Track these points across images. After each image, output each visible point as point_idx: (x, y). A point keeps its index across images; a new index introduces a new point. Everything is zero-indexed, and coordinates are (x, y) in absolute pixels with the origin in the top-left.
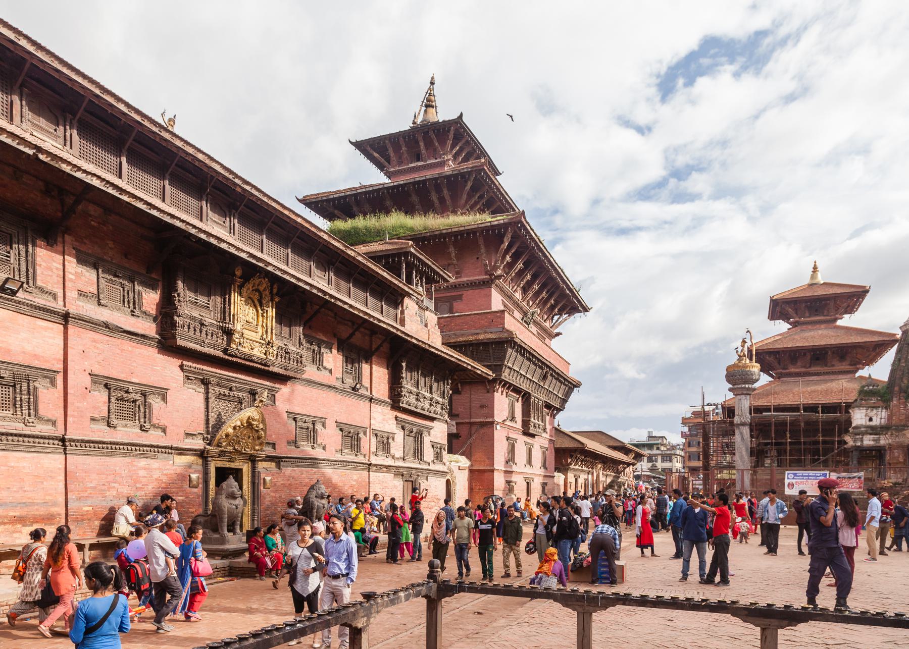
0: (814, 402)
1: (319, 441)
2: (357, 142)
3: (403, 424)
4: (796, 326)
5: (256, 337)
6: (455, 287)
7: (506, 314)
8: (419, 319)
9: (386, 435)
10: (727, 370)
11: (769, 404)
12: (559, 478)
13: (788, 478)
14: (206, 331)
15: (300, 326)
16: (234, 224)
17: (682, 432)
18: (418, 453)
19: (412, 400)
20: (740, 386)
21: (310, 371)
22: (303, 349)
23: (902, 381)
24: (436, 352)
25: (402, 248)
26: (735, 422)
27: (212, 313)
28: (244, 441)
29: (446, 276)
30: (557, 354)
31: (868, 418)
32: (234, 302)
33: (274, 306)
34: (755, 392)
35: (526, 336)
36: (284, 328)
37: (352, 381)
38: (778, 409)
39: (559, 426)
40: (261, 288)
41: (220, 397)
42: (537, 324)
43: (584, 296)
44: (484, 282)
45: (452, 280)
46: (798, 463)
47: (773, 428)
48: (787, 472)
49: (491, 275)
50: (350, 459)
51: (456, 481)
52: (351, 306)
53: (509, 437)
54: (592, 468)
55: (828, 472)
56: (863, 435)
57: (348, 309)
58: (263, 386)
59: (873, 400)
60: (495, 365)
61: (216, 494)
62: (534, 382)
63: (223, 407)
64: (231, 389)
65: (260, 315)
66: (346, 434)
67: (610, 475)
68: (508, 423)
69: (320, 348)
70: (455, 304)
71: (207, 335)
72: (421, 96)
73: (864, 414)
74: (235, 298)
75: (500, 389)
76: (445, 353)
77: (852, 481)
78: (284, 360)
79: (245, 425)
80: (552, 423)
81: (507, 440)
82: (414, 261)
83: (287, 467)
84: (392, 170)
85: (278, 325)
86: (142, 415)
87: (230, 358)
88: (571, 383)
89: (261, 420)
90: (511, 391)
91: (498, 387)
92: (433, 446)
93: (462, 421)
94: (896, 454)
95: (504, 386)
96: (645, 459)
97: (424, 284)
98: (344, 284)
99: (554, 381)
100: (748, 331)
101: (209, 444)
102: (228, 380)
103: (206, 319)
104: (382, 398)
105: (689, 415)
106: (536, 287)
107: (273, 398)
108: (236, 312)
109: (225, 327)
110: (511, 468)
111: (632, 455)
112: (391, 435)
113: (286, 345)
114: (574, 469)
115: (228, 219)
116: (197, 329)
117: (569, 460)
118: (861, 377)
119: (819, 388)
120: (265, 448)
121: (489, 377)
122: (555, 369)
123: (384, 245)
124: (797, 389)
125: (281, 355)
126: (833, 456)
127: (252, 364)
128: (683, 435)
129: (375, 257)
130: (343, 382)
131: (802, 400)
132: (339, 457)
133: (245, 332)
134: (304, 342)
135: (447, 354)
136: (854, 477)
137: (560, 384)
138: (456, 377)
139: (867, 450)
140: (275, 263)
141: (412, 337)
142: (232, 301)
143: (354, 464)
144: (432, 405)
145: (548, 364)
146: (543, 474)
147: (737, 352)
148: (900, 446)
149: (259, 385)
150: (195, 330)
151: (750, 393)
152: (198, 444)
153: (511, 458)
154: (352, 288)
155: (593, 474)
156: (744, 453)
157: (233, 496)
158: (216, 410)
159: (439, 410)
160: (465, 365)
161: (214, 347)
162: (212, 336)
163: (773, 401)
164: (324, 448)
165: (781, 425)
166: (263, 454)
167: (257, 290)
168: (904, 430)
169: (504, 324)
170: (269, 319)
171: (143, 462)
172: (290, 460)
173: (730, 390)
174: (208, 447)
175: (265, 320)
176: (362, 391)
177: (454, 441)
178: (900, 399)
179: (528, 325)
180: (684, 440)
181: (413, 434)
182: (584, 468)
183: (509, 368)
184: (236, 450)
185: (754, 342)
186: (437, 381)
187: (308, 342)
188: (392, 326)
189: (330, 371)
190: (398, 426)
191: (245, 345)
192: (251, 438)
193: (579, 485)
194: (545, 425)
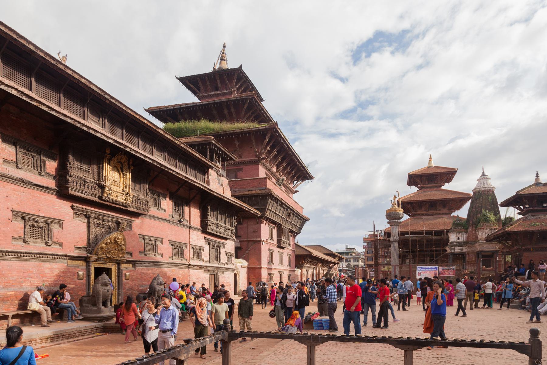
0: (430, 229)
1: (159, 252)
2: (180, 78)
3: (209, 242)
4: (421, 189)
5: (120, 190)
6: (239, 163)
7: (268, 180)
8: (218, 181)
9: (199, 248)
10: (386, 212)
11: (408, 230)
12: (298, 271)
13: (418, 270)
14: (88, 186)
15: (146, 184)
16: (105, 122)
17: (363, 246)
18: (218, 258)
19: (214, 228)
20: (393, 221)
21: (153, 211)
22: (148, 197)
23: (474, 219)
24: (228, 200)
25: (207, 141)
26: (391, 240)
27: (91, 175)
28: (112, 252)
29: (233, 157)
30: (296, 202)
31: (457, 238)
32: (106, 169)
33: (131, 172)
34: (401, 224)
35: (279, 192)
36: (137, 185)
37: (178, 217)
38: (413, 233)
39: (297, 242)
40: (122, 161)
41: (97, 225)
42: (285, 186)
43: (311, 171)
44: (255, 161)
45: (237, 159)
46: (423, 262)
47: (410, 243)
48: (417, 267)
49: (259, 157)
50: (178, 262)
51: (240, 274)
52: (177, 173)
53: (270, 249)
54: (316, 266)
55: (438, 267)
56: (455, 247)
57: (175, 174)
58: (124, 219)
59: (460, 228)
60: (261, 208)
62: (283, 218)
63: (99, 232)
64: (104, 221)
65: (122, 177)
66: (175, 247)
67: (326, 270)
68: (269, 241)
69: (159, 197)
70: (238, 173)
71: (88, 188)
72: (218, 54)
73: (455, 236)
74: (106, 166)
75: (264, 222)
76: (233, 201)
77: (450, 271)
78: (137, 204)
79: (113, 242)
80: (293, 241)
81: (269, 250)
82: (214, 148)
83: (140, 267)
84: (201, 95)
85: (133, 183)
86: (47, 236)
87: (103, 202)
88: (304, 219)
89: (123, 239)
90: (271, 223)
91: (263, 220)
92: (226, 254)
93: (243, 240)
94: (471, 257)
95: (266, 220)
96: (344, 260)
97: (220, 161)
98: (173, 160)
99: (294, 217)
100: (397, 192)
101: (90, 254)
102: (102, 215)
103: (88, 178)
104: (196, 226)
105: (367, 236)
106: (284, 165)
107: (131, 227)
108: (106, 175)
109: (100, 183)
110: (271, 266)
111: (337, 259)
112: (202, 248)
113: (138, 195)
114: (306, 267)
115: (101, 119)
116: (82, 184)
117: (303, 262)
118: (454, 216)
119: (433, 222)
120: (125, 256)
121: (258, 215)
122: (295, 210)
123: (197, 138)
124: (422, 222)
125: (135, 201)
126: (440, 258)
127: (117, 206)
128: (364, 247)
129: (192, 145)
130: (173, 217)
131: (425, 228)
132: (171, 261)
133: (112, 186)
134: (149, 193)
135: (234, 202)
136: (451, 269)
137: (298, 219)
138: (239, 215)
139: (457, 255)
140: (131, 147)
141: (214, 192)
142: (104, 168)
143: (180, 265)
144: (226, 231)
145: (291, 208)
146: (289, 269)
147: (392, 202)
148: (473, 252)
149: (121, 219)
150: (80, 185)
151: (398, 224)
152: (84, 253)
153: (271, 261)
154: (178, 162)
155: (316, 269)
156: (396, 257)
157: (106, 285)
158: (94, 233)
159: (230, 233)
160: (244, 208)
161: (93, 195)
162: (92, 189)
163: (410, 229)
164: (162, 256)
165: (414, 241)
166: (125, 259)
167: (120, 162)
168: (475, 244)
169: (266, 185)
170: (128, 180)
171: (47, 265)
172: (141, 263)
173: (388, 223)
174: (89, 255)
175: (125, 180)
176: (184, 223)
177: (239, 251)
178: (473, 228)
179: (280, 186)
180: (364, 250)
181: (215, 247)
182: (312, 266)
183: (269, 210)
184: (107, 257)
186: (228, 217)
187: (152, 193)
188: (202, 185)
189: (165, 211)
190: (206, 242)
191: (112, 194)
192: (117, 250)
193: (309, 275)
194: (290, 242)
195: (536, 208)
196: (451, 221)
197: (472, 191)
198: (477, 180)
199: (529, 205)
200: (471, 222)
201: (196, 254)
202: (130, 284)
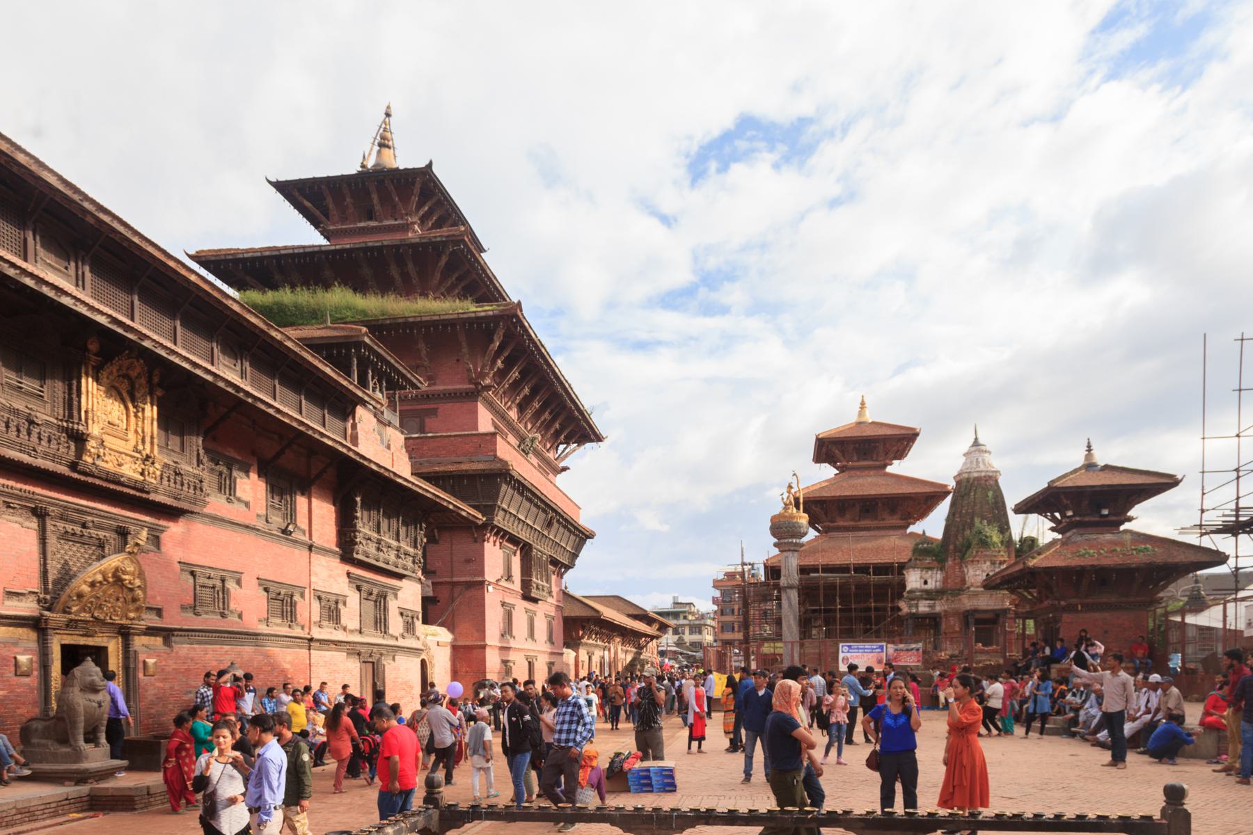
0: (865, 562)
1: (232, 606)
3: (359, 583)
4: (843, 471)
5: (128, 447)
6: (427, 397)
7: (499, 438)
8: (378, 437)
9: (334, 598)
10: (771, 520)
11: (816, 563)
12: (569, 655)
13: (843, 652)
14: (39, 433)
15: (198, 435)
16: (83, 273)
17: (713, 598)
18: (381, 623)
19: (372, 549)
20: (786, 541)
22: (203, 469)
23: (957, 539)
24: (405, 483)
25: (351, 337)
26: (781, 584)
27: (48, 407)
28: (109, 605)
29: (415, 381)
30: (564, 494)
31: (923, 581)
32: (87, 392)
33: (155, 403)
34: (804, 548)
35: (525, 468)
36: (171, 436)
37: (280, 520)
38: (828, 569)
39: (566, 588)
40: (133, 374)
41: (65, 536)
42: (538, 454)
43: (599, 421)
45: (424, 386)
46: (850, 635)
47: (822, 591)
48: (841, 645)
49: (477, 384)
50: (281, 631)
51: (434, 661)
52: (278, 411)
53: (504, 603)
54: (609, 643)
55: (884, 644)
56: (918, 601)
57: (274, 414)
58: (139, 523)
59: (928, 560)
60: (485, 506)
61: (64, 685)
62: (536, 529)
63: (71, 553)
64: (84, 526)
65: (132, 414)
66: (274, 595)
67: (631, 651)
68: (503, 583)
69: (230, 469)
70: (427, 420)
71: (40, 439)
73: (918, 576)
74: (89, 385)
75: (492, 538)
76: (417, 486)
77: (910, 653)
78: (172, 485)
79: (111, 580)
80: (559, 584)
81: (503, 605)
82: (369, 356)
83: (182, 643)
85: (163, 433)
87: (83, 478)
88: (583, 533)
89: (137, 572)
90: (507, 541)
91: (489, 535)
92: (402, 614)
93: (440, 580)
94: (952, 622)
95: (496, 534)
96: (670, 630)
97: (384, 389)
98: (266, 380)
99: (562, 530)
100: (794, 475)
101: (49, 609)
103: (38, 414)
104: (326, 545)
105: (721, 577)
106: (536, 405)
107: (156, 540)
108: (90, 406)
109: (73, 429)
110: (508, 642)
111: (656, 626)
112: (341, 599)
113: (176, 463)
114: (586, 644)
115: (73, 264)
116: (22, 429)
117: (581, 633)
118: (912, 534)
119: (869, 545)
120: (144, 616)
121: (477, 521)
122: (562, 513)
123: (324, 331)
124: (846, 546)
125: (169, 477)
126: (885, 625)
127: (119, 488)
128: (715, 601)
129: (315, 346)
130: (267, 521)
131: (853, 560)
133: (105, 437)
134: (205, 460)
135: (420, 487)
136: (912, 649)
137: (568, 534)
138: (431, 520)
139: (926, 618)
140: (155, 337)
141: (370, 461)
142: (83, 389)
143: (287, 639)
144: (400, 557)
145: (554, 506)
146: (549, 650)
147: (783, 499)
148: (956, 613)
149: (132, 521)
150: (18, 431)
151: (796, 548)
152: (27, 608)
153: (508, 630)
154: (278, 386)
155: (609, 650)
156: (792, 622)
157: (93, 689)
158: (59, 556)
159: (410, 564)
160: (445, 504)
161: (54, 458)
162: (49, 441)
163: (821, 560)
164: (240, 616)
165: (831, 587)
166: (142, 625)
167: (126, 376)
168: (959, 594)
169: (495, 451)
170: (148, 422)
173: (776, 545)
175: (140, 423)
176: (296, 535)
177: (430, 607)
178: (955, 559)
179: (527, 454)
180: (715, 608)
182: (599, 643)
183: (504, 510)
184: (95, 618)
185: (801, 487)
186: (405, 524)
187: (212, 460)
188: (341, 444)
190: (351, 585)
191: (107, 458)
192: (122, 600)
193: (594, 664)
194: (551, 587)
195: (1087, 519)
196: (909, 544)
197: (954, 477)
198: (964, 455)
199: (1074, 512)
200: (951, 547)
201: (326, 613)
202: (158, 688)
